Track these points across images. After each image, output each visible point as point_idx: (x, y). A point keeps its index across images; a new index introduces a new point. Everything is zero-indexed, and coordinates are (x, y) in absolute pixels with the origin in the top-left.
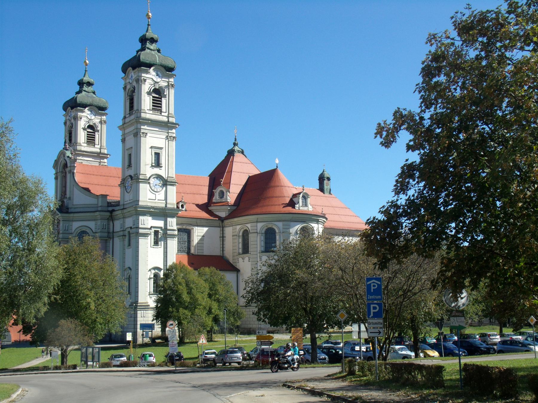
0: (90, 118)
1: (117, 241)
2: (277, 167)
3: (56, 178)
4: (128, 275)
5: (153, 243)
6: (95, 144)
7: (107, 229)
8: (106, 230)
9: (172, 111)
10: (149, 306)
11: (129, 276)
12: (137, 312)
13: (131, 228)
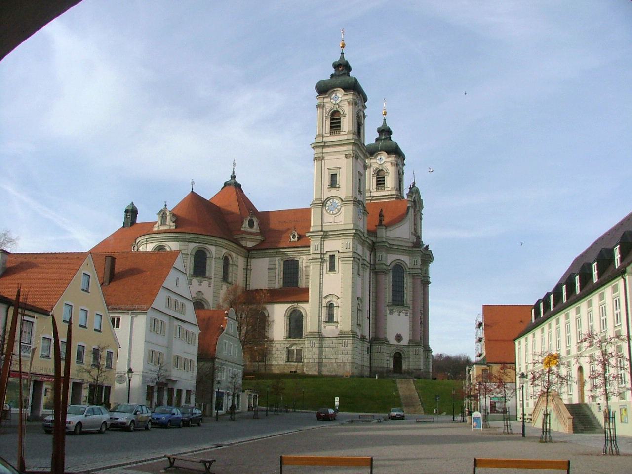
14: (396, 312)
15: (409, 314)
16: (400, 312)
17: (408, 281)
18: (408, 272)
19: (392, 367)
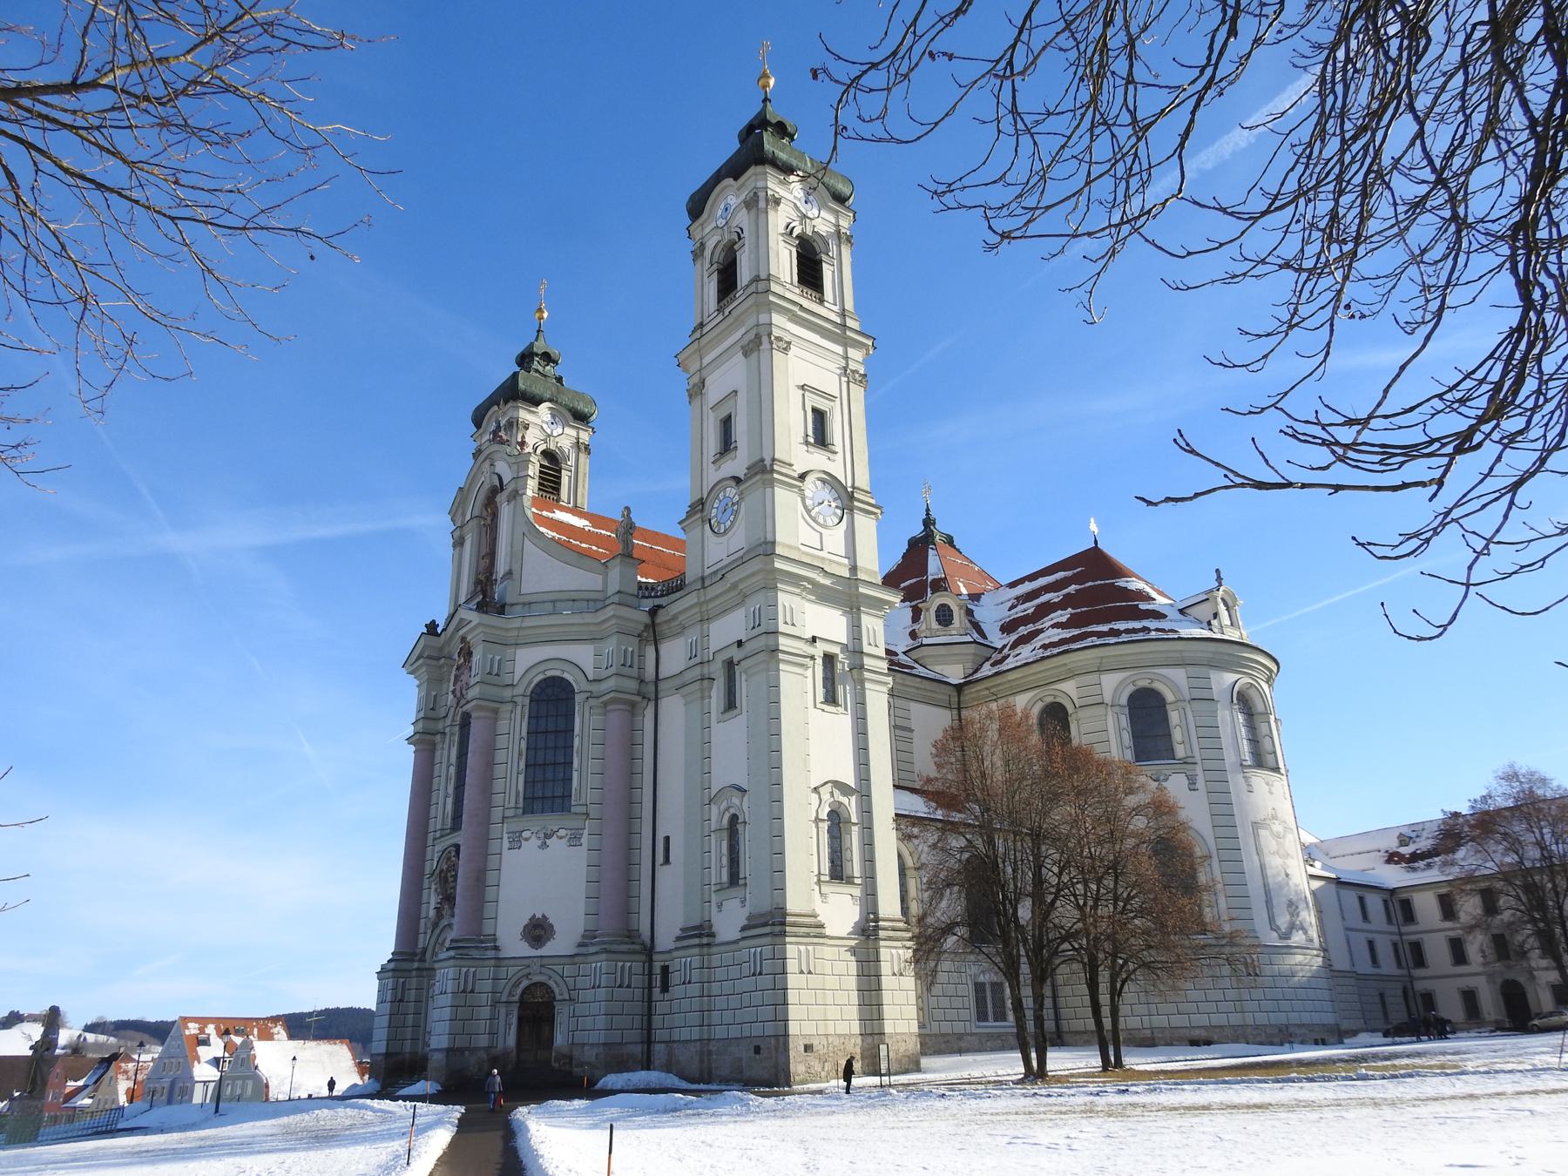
0: (549, 431)
1: (673, 708)
2: (1096, 542)
3: (459, 543)
4: (727, 816)
5: (820, 697)
6: (558, 500)
7: (636, 666)
8: (634, 672)
9: (849, 305)
10: (822, 926)
11: (734, 818)
12: (784, 951)
13: (740, 643)
14: (534, 836)
15: (584, 840)
16: (547, 836)
17: (587, 725)
18: (583, 696)
19: (511, 1041)
